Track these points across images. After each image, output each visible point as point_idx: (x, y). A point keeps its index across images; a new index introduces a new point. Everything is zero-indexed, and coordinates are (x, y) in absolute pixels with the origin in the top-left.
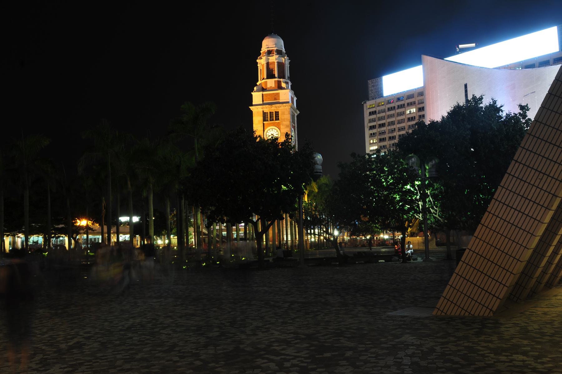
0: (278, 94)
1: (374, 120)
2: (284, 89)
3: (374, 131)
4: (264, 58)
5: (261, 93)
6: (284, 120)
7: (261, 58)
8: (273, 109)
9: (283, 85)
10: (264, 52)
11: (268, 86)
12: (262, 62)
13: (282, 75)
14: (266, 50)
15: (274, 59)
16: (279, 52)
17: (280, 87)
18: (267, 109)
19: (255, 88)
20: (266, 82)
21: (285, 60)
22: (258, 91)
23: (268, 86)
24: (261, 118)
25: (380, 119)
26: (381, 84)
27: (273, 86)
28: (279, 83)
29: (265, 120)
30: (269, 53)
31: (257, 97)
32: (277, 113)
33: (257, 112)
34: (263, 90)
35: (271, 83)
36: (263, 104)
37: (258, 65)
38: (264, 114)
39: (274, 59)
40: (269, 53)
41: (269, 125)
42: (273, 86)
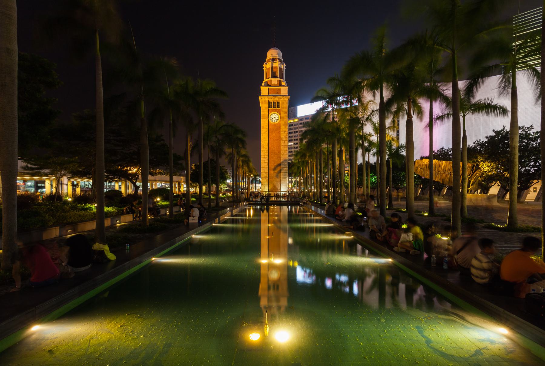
0: (280, 89)
1: (292, 129)
2: (284, 86)
3: (292, 135)
4: (270, 63)
5: (268, 87)
6: (283, 108)
7: (266, 64)
8: (276, 99)
9: (283, 84)
10: (269, 61)
11: (273, 83)
12: (267, 66)
13: (281, 77)
14: (271, 57)
15: (277, 64)
16: (280, 60)
17: (281, 85)
18: (272, 99)
19: (263, 84)
20: (271, 80)
21: (283, 66)
22: (264, 86)
23: (273, 83)
24: (267, 105)
25: (295, 129)
26: (297, 110)
27: (276, 83)
28: (280, 81)
29: (269, 107)
30: (273, 60)
31: (264, 90)
32: (278, 103)
33: (263, 102)
34: (268, 85)
35: (275, 81)
36: (269, 96)
37: (264, 69)
38: (270, 103)
39: (277, 64)
40: (273, 60)
41: (273, 111)
42: (276, 83)
